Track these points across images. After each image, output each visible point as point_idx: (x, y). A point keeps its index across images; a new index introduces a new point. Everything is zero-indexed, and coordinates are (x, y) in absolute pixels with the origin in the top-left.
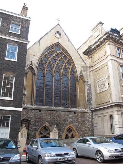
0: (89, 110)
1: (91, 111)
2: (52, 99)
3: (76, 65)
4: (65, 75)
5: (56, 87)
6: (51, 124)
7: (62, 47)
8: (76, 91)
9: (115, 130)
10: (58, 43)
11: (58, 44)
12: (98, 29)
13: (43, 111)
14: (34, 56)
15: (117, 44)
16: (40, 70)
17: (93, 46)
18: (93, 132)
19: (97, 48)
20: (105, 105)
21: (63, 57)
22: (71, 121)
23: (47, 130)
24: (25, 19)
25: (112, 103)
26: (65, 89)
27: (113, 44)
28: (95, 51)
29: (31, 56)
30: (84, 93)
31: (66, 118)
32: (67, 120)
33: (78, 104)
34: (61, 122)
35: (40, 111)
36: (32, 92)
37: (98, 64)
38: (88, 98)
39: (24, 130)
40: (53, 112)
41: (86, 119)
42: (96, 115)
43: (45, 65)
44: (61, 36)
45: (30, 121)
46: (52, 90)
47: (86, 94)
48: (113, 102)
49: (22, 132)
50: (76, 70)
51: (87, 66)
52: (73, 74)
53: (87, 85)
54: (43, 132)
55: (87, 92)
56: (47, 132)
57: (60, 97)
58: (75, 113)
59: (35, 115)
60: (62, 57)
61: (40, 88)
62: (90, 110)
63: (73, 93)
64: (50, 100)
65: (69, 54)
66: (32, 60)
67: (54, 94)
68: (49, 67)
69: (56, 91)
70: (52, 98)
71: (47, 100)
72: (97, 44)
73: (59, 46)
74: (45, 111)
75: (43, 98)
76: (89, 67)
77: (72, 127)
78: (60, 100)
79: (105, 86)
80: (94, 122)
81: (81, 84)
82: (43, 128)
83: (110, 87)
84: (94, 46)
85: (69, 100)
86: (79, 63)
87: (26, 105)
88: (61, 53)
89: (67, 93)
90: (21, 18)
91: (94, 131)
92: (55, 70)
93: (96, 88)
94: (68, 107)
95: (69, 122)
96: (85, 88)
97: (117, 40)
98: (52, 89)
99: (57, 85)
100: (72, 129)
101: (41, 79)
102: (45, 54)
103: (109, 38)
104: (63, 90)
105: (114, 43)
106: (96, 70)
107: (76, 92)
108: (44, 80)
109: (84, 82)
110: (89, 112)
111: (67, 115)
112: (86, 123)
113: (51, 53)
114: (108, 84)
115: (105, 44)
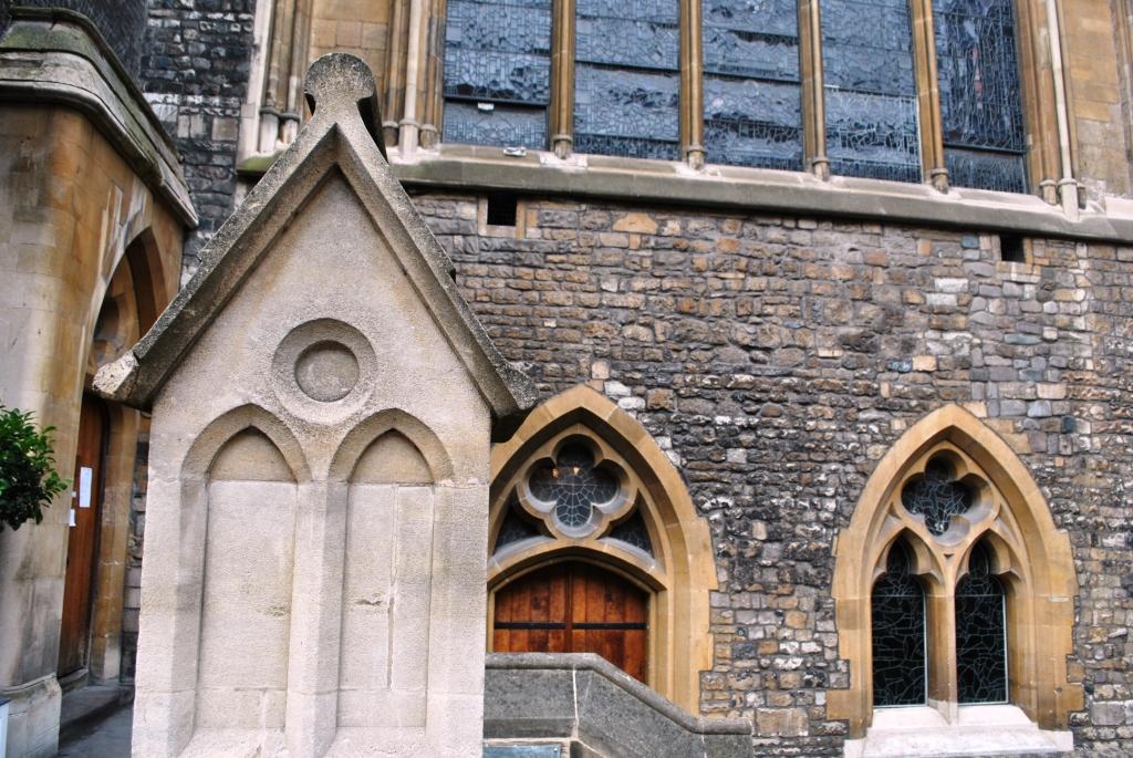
13: (551, 209)
22: (965, 364)
23: (609, 479)
31: (892, 317)
32: (908, 347)
34: (814, 361)
35: (503, 207)
40: (694, 224)
54: (540, 506)
56: (614, 507)
58: (1013, 241)
74: (565, 213)
82: (547, 451)
94: (913, 176)
95: (938, 372)
100: (971, 467)
111: (897, 281)
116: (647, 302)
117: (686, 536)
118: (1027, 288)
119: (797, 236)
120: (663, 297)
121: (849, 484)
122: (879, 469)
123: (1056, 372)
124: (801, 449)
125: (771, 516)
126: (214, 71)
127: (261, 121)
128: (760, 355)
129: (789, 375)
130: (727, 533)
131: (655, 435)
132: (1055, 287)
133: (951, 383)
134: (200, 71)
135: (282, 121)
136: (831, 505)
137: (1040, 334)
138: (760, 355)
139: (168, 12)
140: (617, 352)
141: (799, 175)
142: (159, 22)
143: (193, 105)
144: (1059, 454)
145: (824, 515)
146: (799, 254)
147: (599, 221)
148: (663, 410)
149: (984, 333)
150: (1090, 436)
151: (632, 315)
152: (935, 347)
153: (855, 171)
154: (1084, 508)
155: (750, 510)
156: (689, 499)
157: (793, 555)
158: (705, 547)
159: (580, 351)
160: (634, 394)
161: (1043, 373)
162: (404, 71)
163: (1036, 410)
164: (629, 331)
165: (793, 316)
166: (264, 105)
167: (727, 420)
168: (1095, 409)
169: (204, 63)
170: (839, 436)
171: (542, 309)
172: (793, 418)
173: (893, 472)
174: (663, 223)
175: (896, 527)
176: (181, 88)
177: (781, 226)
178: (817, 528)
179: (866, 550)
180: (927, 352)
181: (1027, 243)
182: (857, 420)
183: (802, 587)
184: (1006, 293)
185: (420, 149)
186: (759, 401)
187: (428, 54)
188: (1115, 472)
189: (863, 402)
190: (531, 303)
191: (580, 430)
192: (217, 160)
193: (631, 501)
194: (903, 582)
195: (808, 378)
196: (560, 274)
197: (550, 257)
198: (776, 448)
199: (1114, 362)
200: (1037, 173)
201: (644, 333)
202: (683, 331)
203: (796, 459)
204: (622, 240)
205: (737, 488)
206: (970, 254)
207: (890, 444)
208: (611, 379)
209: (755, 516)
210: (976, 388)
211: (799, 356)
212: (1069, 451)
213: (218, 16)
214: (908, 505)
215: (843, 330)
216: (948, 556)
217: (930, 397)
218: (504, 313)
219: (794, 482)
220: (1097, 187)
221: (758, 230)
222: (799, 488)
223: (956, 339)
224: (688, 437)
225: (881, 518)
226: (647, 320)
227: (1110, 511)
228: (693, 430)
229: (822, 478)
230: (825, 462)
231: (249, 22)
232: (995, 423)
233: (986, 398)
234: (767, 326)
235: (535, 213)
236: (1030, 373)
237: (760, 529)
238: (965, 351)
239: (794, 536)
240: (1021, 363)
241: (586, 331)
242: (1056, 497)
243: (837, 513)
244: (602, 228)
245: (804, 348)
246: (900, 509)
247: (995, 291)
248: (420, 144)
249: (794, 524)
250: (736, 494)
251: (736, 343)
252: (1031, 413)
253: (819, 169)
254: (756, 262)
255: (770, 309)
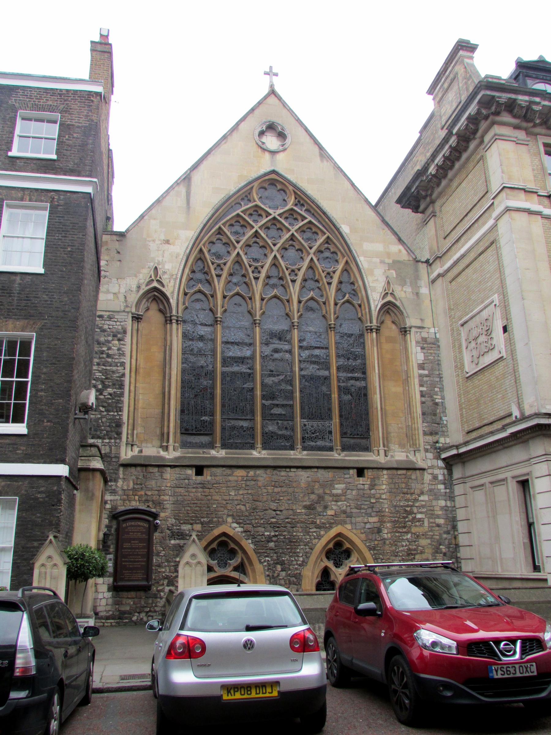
0: (430, 455)
1: (444, 460)
2: (253, 420)
3: (362, 260)
4: (312, 309)
5: (272, 366)
6: (249, 527)
7: (291, 188)
8: (364, 373)
9: (545, 554)
10: (274, 172)
11: (273, 176)
12: (452, 76)
13: (214, 470)
14: (167, 242)
15: (544, 131)
16: (197, 300)
17: (433, 161)
18: (457, 558)
19: (452, 167)
20: (492, 433)
21: (301, 230)
22: (344, 512)
23: (233, 553)
24: (75, 92)
25: (524, 418)
26: (312, 370)
27: (521, 135)
28: (444, 183)
29: (153, 246)
30: (406, 381)
31: (321, 498)
32: (326, 507)
33: (377, 431)
34: (295, 514)
35: (199, 470)
36: (164, 396)
37: (463, 240)
38: (423, 403)
39: (50, 557)
40: (259, 472)
41: (416, 500)
42: (464, 480)
43: (219, 276)
44: (288, 141)
45: (155, 516)
46: (253, 380)
47: (417, 386)
48: (527, 413)
49: (43, 565)
50: (360, 283)
51: (418, 259)
52: (348, 301)
53: (417, 342)
55: (420, 376)
56: (234, 562)
57: (292, 406)
59: (177, 490)
60: (293, 231)
61: (198, 377)
62: (438, 457)
63: (352, 382)
64: (245, 424)
65: (324, 213)
66: (160, 259)
67: (263, 397)
68: (235, 280)
69: (269, 381)
70: (253, 412)
71: (233, 422)
72: (446, 150)
73: (279, 187)
74: (219, 471)
75: (212, 414)
76: (427, 262)
77: (347, 538)
78: (292, 418)
79: (494, 342)
80: (461, 514)
81: (390, 340)
82: (214, 545)
83: (510, 342)
84: (436, 162)
85: (334, 418)
86: (379, 247)
87: (136, 450)
88: (291, 214)
89: (324, 389)
90: (61, 90)
91: (463, 553)
92: (263, 291)
93: (460, 352)
94: (331, 449)
95: (336, 515)
96: (407, 358)
97: (540, 112)
98: (250, 376)
99: (276, 356)
100: (347, 545)
101: (201, 338)
102: (217, 227)
103: (493, 109)
104: (303, 373)
105: (526, 129)
106: (455, 271)
107: (365, 379)
108: (213, 341)
109: (404, 331)
110: (432, 467)
111: (323, 486)
112: (419, 516)
113: (244, 220)
114: (505, 329)
115: (482, 142)
116: (243, 498)
117: (256, 570)
118: (366, 486)
119: (291, 474)
120: (248, 496)
121: (307, 552)
122: (316, 548)
123: (375, 513)
124: (291, 542)
125: (282, 563)
126: (112, 431)
127: (126, 446)
128: (278, 512)
129: (288, 518)
130: (268, 569)
131: (247, 539)
132: (375, 485)
133: (340, 518)
134: (107, 432)
135: (132, 445)
136: (301, 559)
137: (370, 501)
138: (278, 512)
139: (97, 413)
140: (235, 514)
141: (292, 452)
142: (94, 416)
143: (106, 443)
144: (376, 540)
145: (299, 562)
146: (291, 480)
147: (229, 473)
148: (249, 531)
149: (351, 502)
150: (387, 534)
151: (239, 502)
152: (334, 507)
153: (312, 449)
154: (385, 558)
155: (275, 562)
156: (257, 559)
157: (289, 575)
158: (262, 573)
159: (224, 514)
160: (240, 527)
161: (370, 514)
162: (168, 427)
163: (368, 526)
164: (238, 507)
165: (289, 500)
166: (127, 441)
167: (268, 533)
168: (388, 525)
169: (108, 429)
170: (304, 537)
171: (212, 501)
172: (289, 532)
173: (321, 548)
174: (248, 472)
175: (323, 565)
176: (103, 438)
177: (285, 471)
178: (296, 566)
179: (313, 573)
180: (332, 509)
181: (366, 471)
182: (309, 532)
183: (292, 585)
184: (359, 488)
185: (174, 452)
186: (278, 527)
187: (176, 420)
188: (396, 545)
189: (311, 526)
190: (209, 500)
191: (224, 538)
192: (114, 460)
193: (240, 560)
194: (328, 583)
195: (294, 519)
196: (217, 490)
197: (214, 485)
198: (283, 542)
199: (395, 509)
200: (373, 445)
201: (243, 508)
202: (255, 506)
203: (290, 545)
204: (236, 478)
205: (272, 555)
206: (346, 476)
207: (320, 539)
208: (233, 522)
209: (277, 563)
210: (348, 520)
211: (291, 512)
212: (379, 539)
213: (112, 413)
214: (328, 558)
215: (305, 503)
216: (340, 574)
217: (333, 523)
218: (200, 503)
219: (289, 552)
220: (394, 447)
221: (278, 473)
222: (291, 554)
223: (341, 505)
224: (257, 540)
225: (318, 563)
226: (244, 503)
227: (394, 558)
228: (258, 537)
229: (298, 550)
230: (299, 545)
231: (121, 415)
232: (354, 531)
233: (351, 523)
234: (281, 503)
235: (209, 472)
236: (366, 514)
237: (279, 567)
238: (345, 508)
239: (290, 569)
240: (363, 511)
241: (225, 507)
242: (375, 554)
243: (303, 561)
244: (230, 475)
245: (292, 510)
246: (325, 559)
247: (355, 488)
248: (174, 450)
249: (289, 565)
250: (271, 557)
251: (271, 509)
252: (367, 527)
253: (298, 450)
254: (277, 483)
255: (282, 498)
